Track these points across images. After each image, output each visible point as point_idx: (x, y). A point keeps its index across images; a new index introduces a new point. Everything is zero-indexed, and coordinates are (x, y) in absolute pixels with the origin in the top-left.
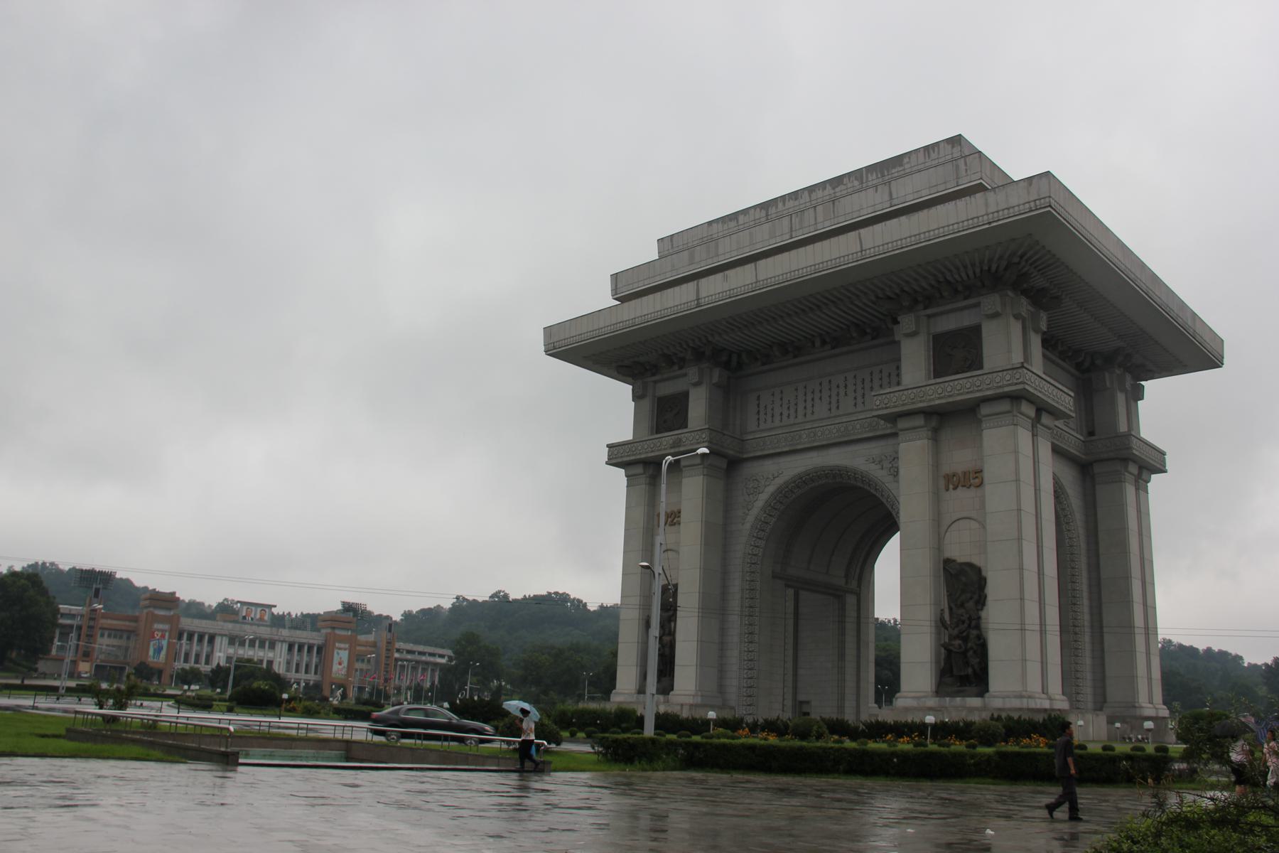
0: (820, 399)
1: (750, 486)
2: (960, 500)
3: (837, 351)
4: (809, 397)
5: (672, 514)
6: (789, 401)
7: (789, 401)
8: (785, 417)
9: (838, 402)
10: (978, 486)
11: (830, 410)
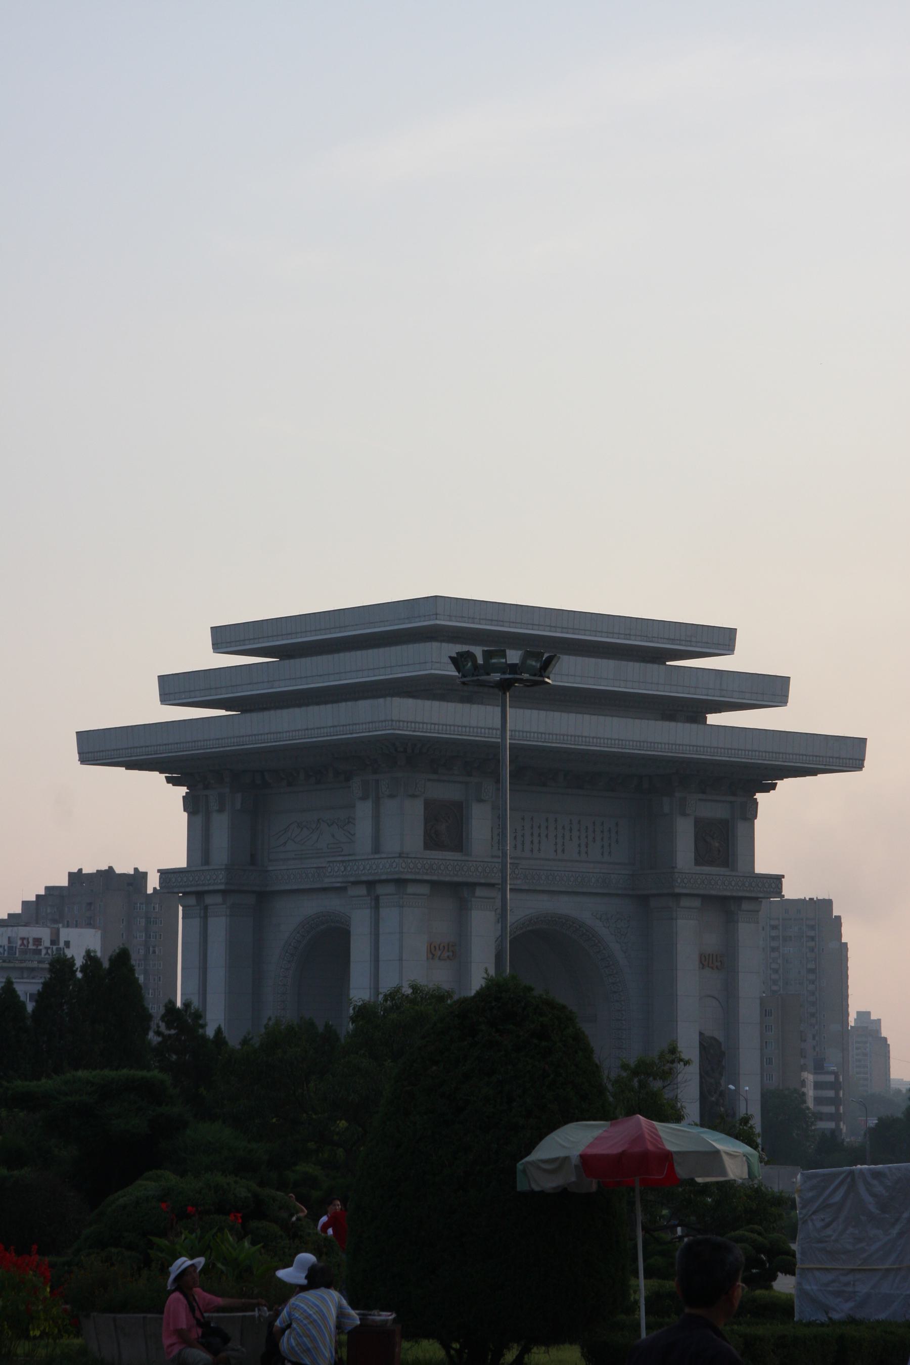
0: (547, 836)
6: (516, 830)
7: (516, 830)
9: (563, 845)
11: (556, 851)
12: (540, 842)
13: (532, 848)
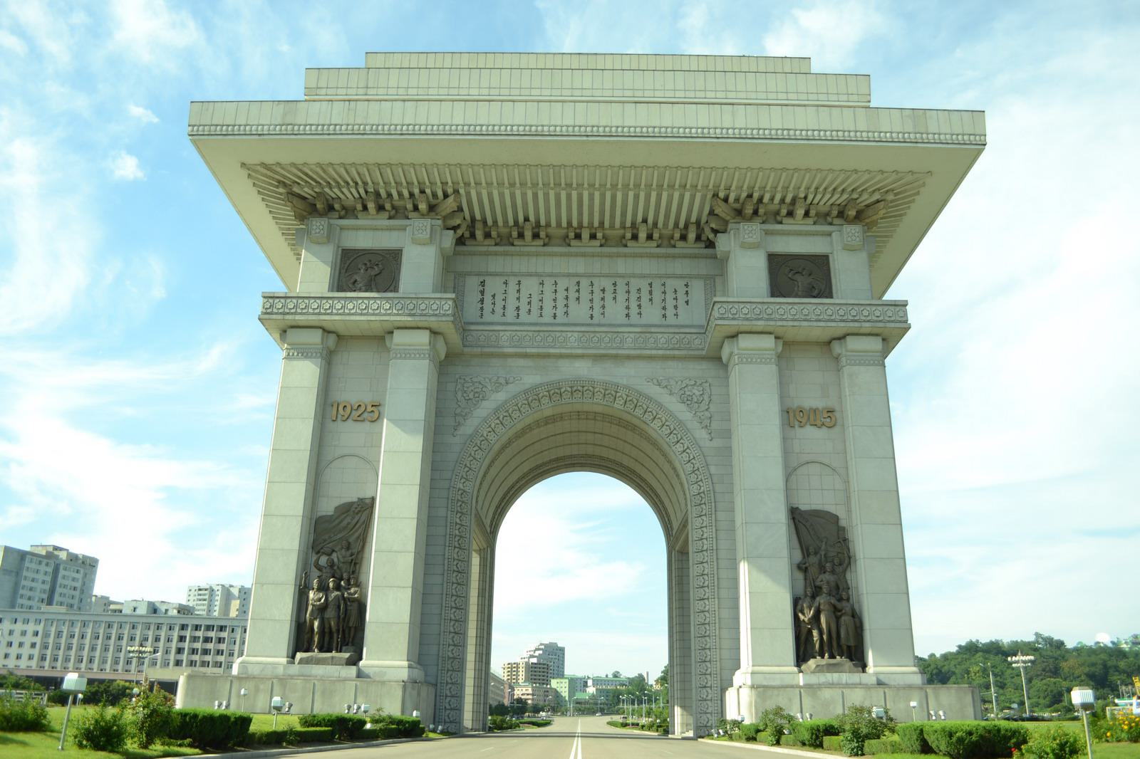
0: (578, 299)
1: (470, 389)
2: (811, 438)
3: (605, 250)
4: (561, 295)
5: (360, 406)
7: (530, 295)
8: (523, 312)
10: (829, 427)
12: (566, 306)
13: (555, 314)
